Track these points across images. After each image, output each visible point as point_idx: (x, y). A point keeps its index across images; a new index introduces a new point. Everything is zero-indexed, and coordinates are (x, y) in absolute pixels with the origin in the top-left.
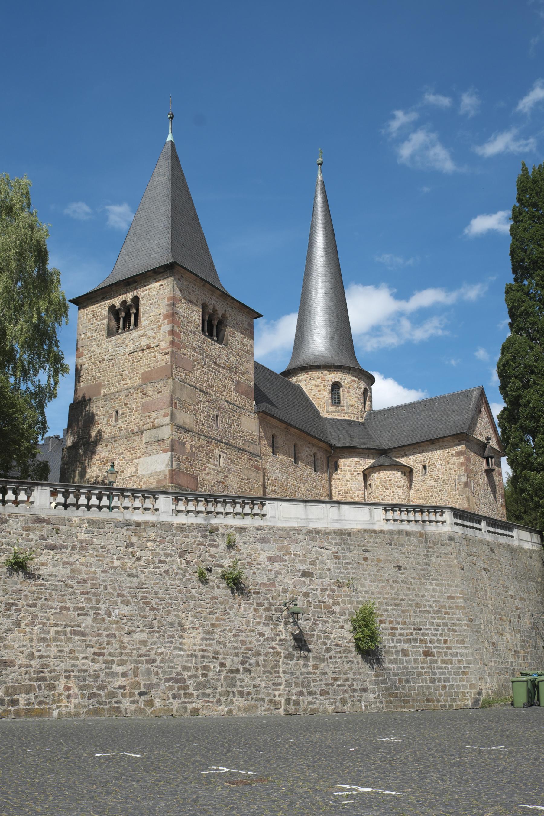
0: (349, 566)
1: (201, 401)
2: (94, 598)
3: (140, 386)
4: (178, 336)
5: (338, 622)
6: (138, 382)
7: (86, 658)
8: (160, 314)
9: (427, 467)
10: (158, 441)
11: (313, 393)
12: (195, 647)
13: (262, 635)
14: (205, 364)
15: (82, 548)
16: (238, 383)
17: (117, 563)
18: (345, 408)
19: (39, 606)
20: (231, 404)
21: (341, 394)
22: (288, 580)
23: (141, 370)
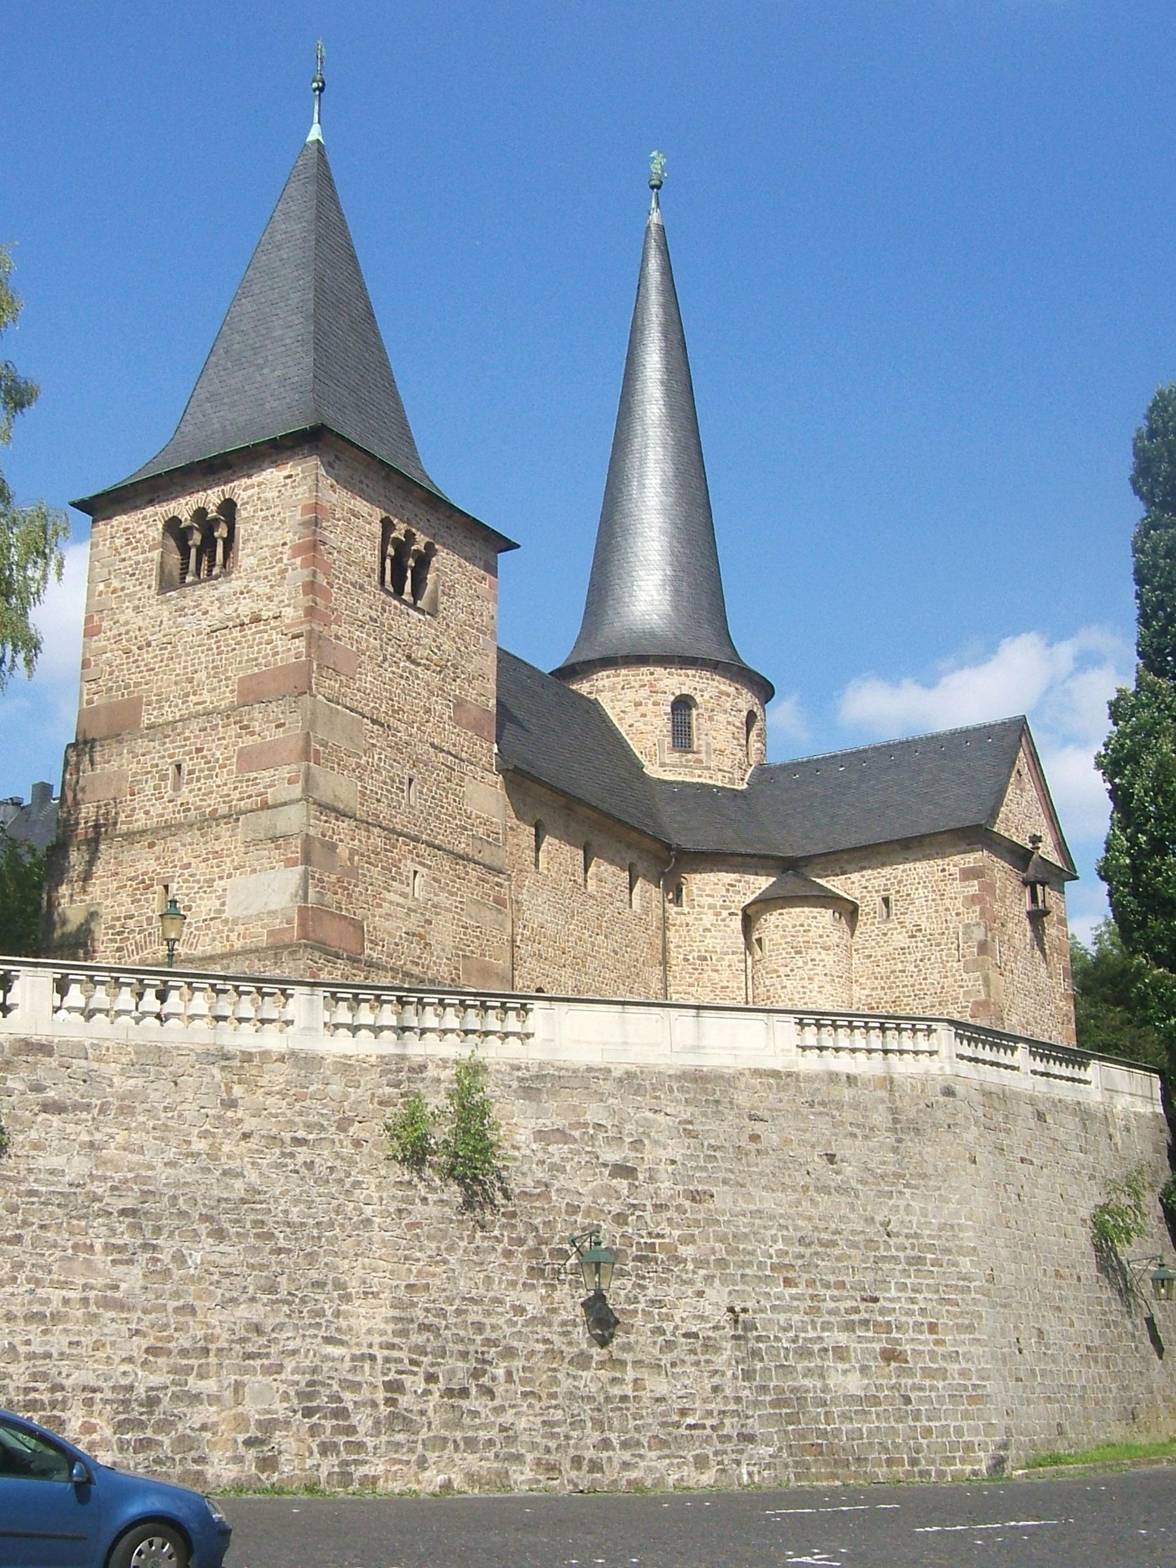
0: (718, 1154)
1: (374, 745)
2: (147, 1225)
3: (234, 709)
4: (327, 596)
5: (690, 1282)
6: (228, 698)
7: (130, 1360)
8: (284, 544)
9: (892, 904)
10: (274, 839)
12: (370, 1339)
13: (520, 1310)
14: (385, 659)
15: (122, 1110)
16: (459, 704)
17: (199, 1145)
18: (703, 756)
19: (27, 1240)
20: (442, 751)
21: (694, 724)
22: (583, 1185)
23: (236, 674)
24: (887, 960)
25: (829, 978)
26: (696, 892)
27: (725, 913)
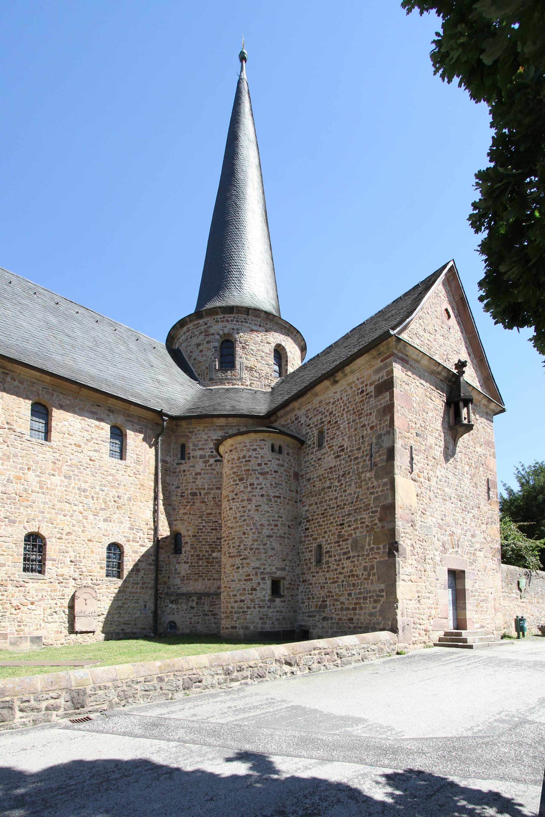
24: (320, 480)
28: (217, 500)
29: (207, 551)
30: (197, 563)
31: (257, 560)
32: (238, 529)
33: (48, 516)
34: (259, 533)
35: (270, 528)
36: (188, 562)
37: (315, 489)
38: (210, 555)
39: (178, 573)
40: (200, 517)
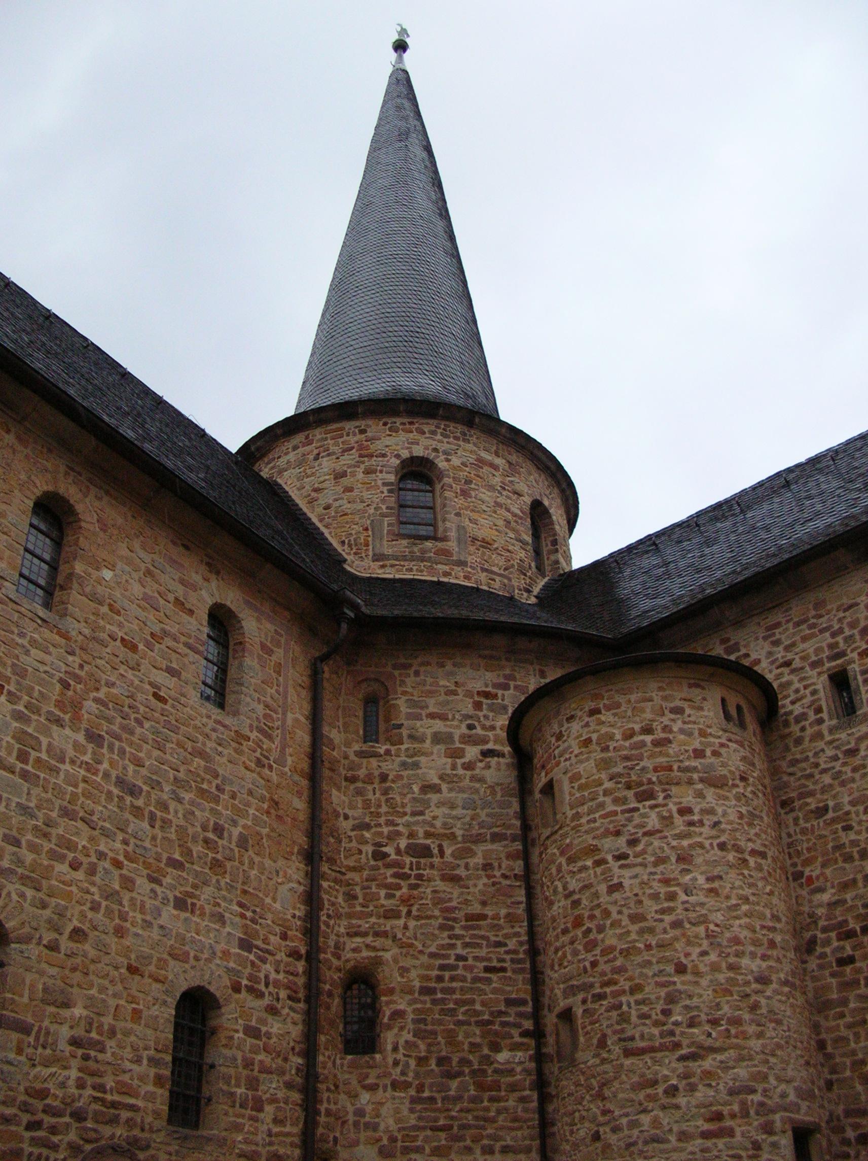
11: (325, 498)
18: (452, 545)
25: (731, 856)
26: (404, 709)
27: (472, 752)
28: (497, 873)
29: (474, 1047)
30: (443, 1088)
31: (741, 1059)
32: (653, 956)
33: (29, 857)
34: (731, 967)
35: (760, 951)
36: (407, 1085)
37: (852, 836)
38: (487, 1060)
39: (367, 1125)
40: (442, 927)
